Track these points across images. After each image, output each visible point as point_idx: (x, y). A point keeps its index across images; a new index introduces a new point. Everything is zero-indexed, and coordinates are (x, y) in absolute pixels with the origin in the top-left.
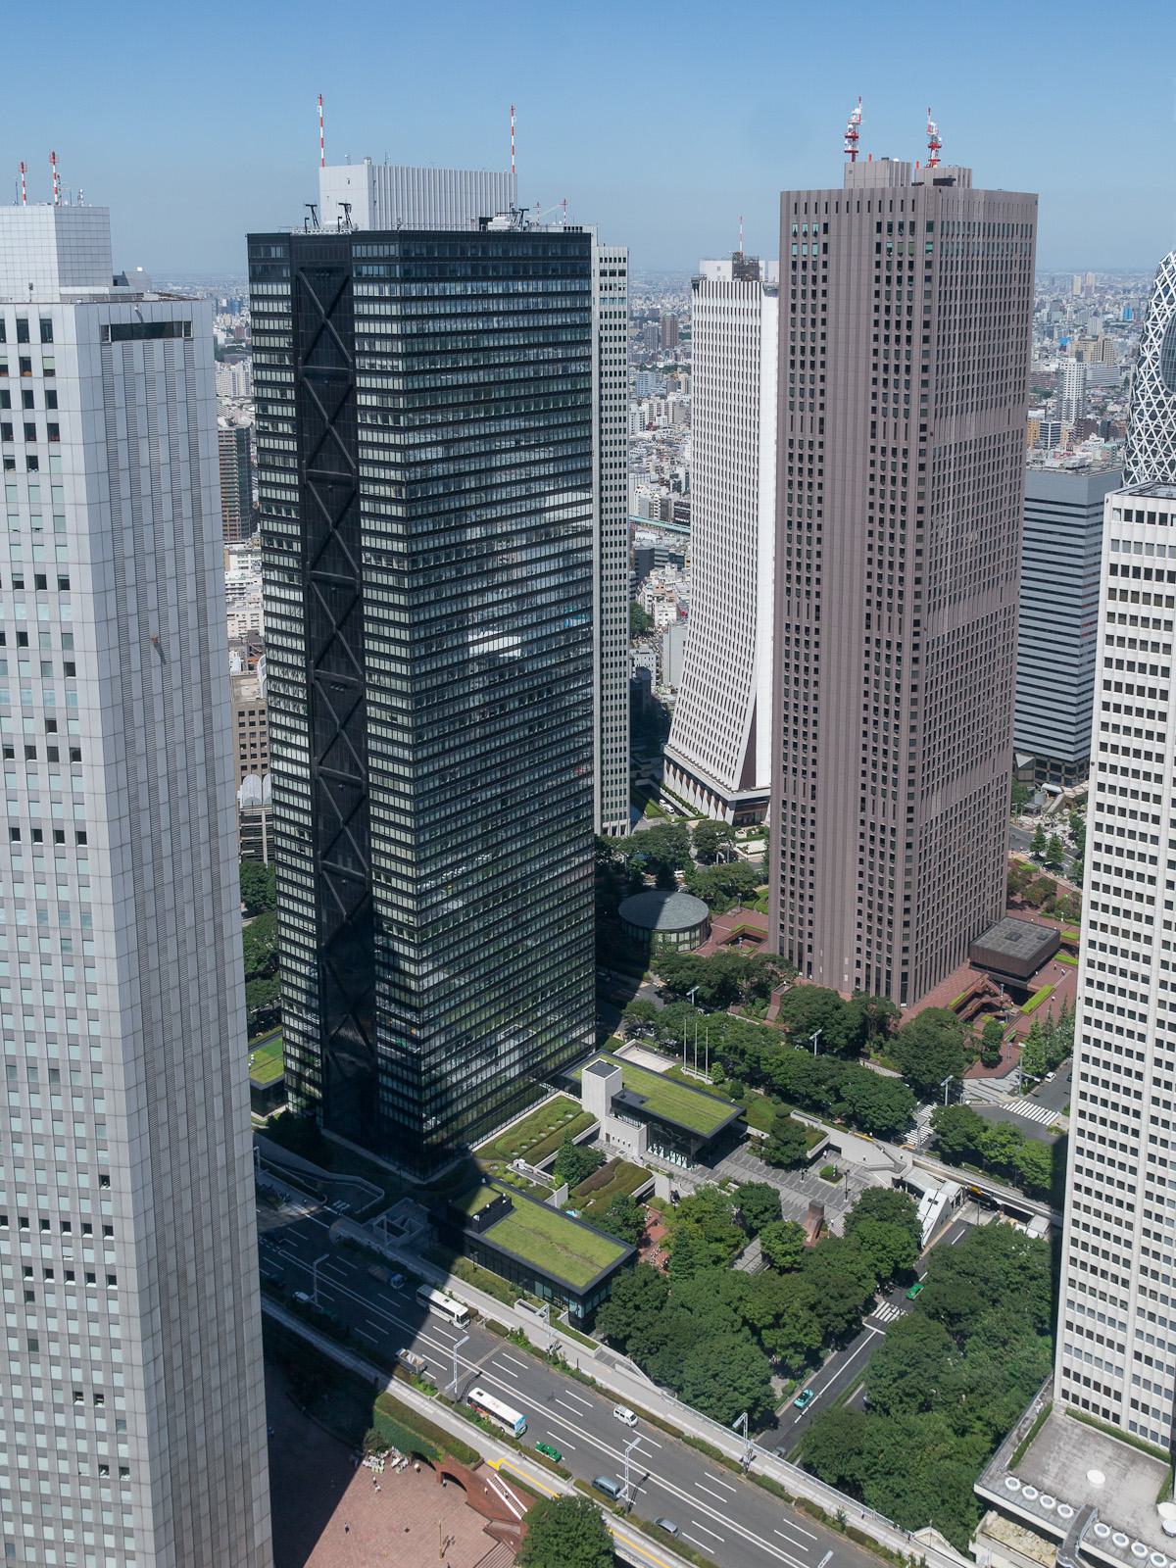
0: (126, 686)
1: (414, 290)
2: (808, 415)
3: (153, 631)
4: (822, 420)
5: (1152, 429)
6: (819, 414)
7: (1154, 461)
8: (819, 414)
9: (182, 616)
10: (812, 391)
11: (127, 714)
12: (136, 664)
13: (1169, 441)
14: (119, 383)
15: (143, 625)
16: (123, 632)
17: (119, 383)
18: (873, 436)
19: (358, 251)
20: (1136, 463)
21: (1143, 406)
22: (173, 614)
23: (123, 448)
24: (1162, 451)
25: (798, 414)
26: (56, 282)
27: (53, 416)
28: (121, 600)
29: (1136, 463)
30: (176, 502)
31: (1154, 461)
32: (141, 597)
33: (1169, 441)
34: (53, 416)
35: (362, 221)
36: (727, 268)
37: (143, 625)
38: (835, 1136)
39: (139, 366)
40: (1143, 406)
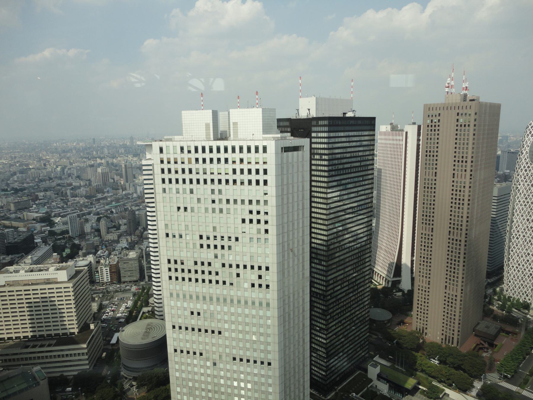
0: (283, 265)
1: (332, 134)
2: (431, 171)
3: (291, 247)
4: (436, 173)
5: (525, 174)
6: (435, 171)
7: (526, 184)
8: (435, 171)
9: (298, 241)
10: (433, 164)
11: (284, 273)
12: (286, 258)
13: (531, 178)
14: (285, 166)
15: (288, 245)
16: (283, 247)
17: (285, 166)
18: (453, 177)
19: (314, 123)
20: (520, 185)
21: (522, 168)
22: (296, 241)
23: (285, 187)
24: (529, 181)
25: (427, 171)
26: (262, 133)
27: (265, 177)
28: (283, 237)
29: (520, 185)
30: (298, 205)
31: (526, 184)
32: (288, 236)
33: (531, 178)
34: (265, 177)
35: (313, 114)
36: (389, 127)
37: (288, 245)
38: (447, 391)
39: (290, 160)
40: (522, 168)
